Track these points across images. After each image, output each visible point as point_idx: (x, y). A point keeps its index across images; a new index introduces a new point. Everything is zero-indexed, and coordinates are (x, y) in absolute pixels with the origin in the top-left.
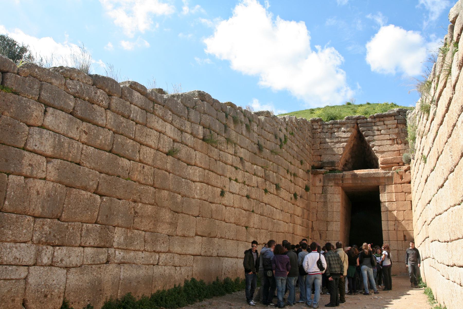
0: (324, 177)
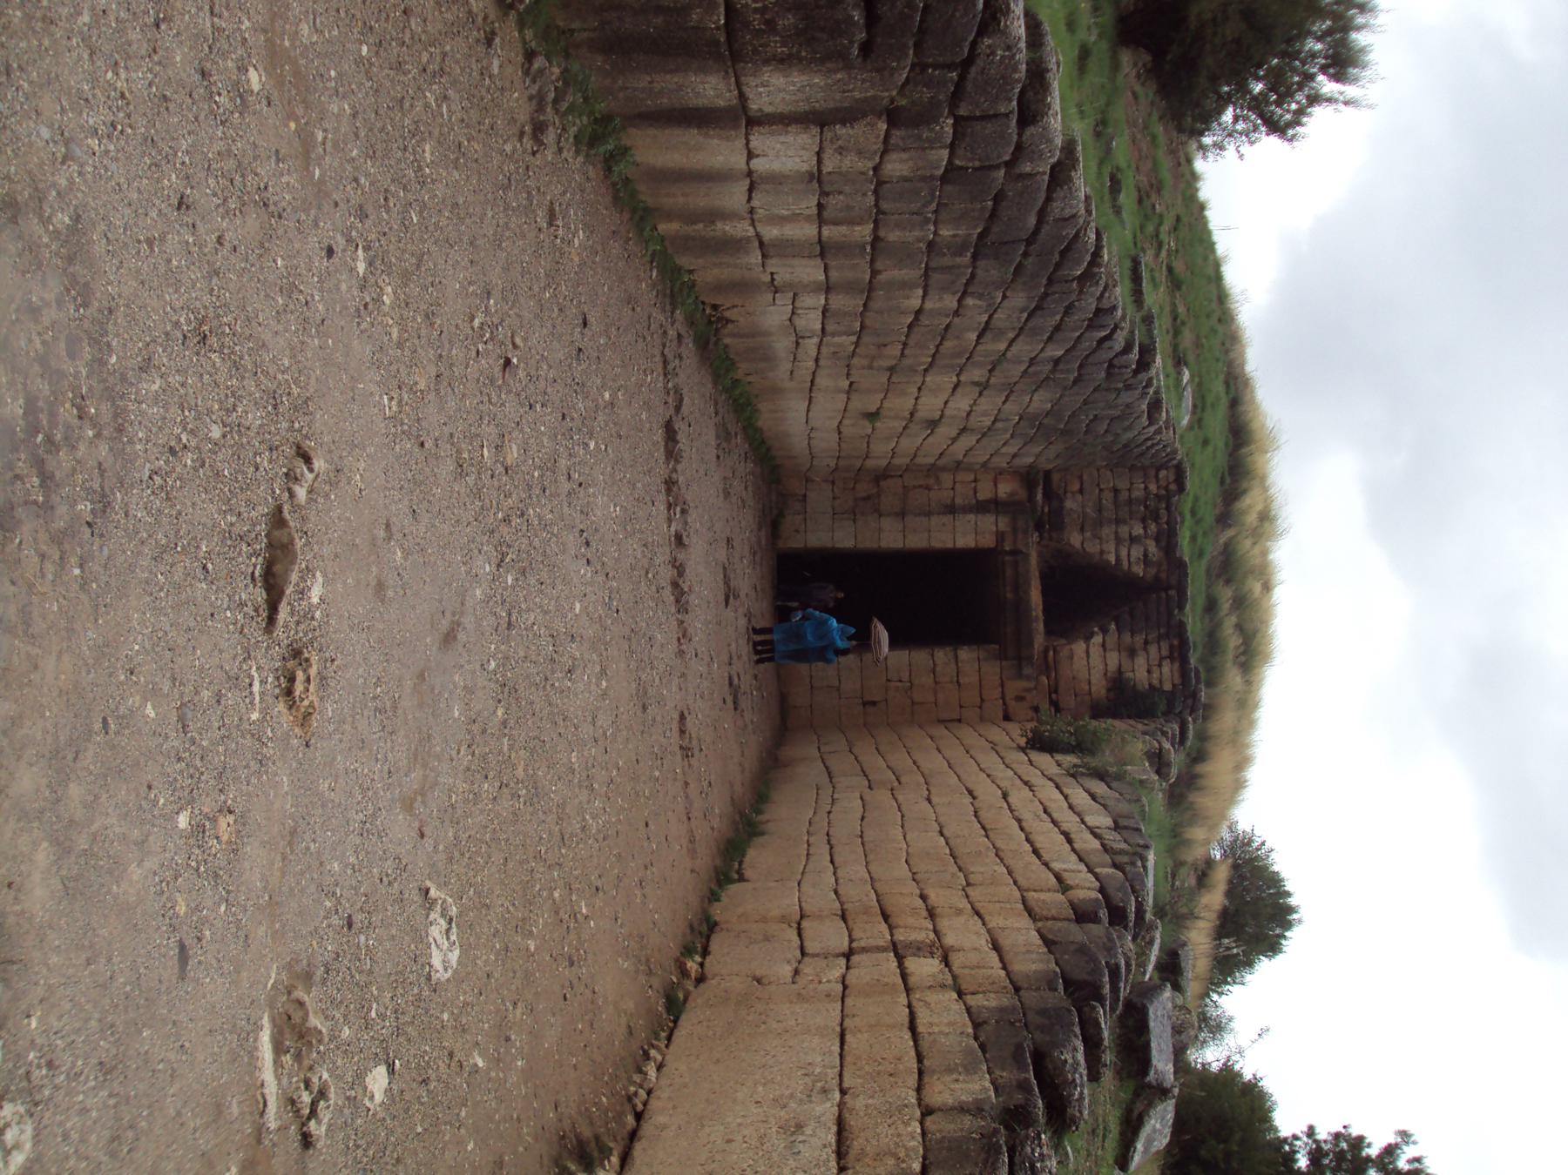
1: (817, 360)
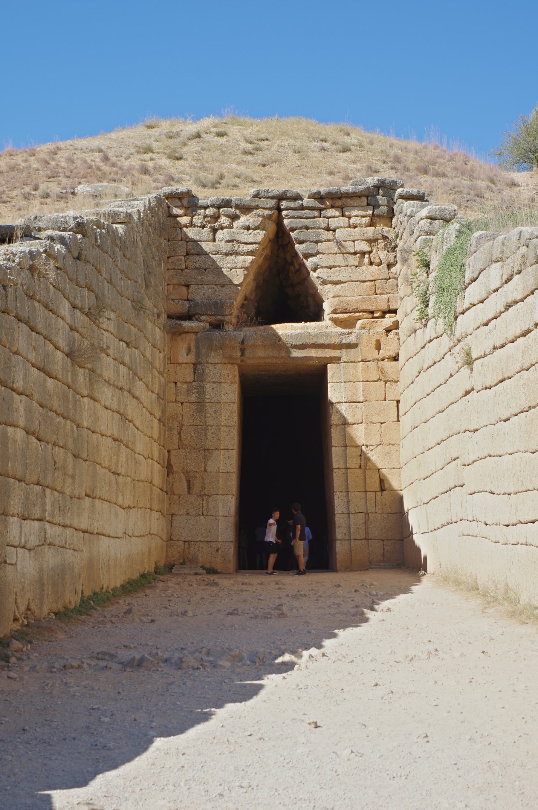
0: (197, 341)
1: (64, 526)
